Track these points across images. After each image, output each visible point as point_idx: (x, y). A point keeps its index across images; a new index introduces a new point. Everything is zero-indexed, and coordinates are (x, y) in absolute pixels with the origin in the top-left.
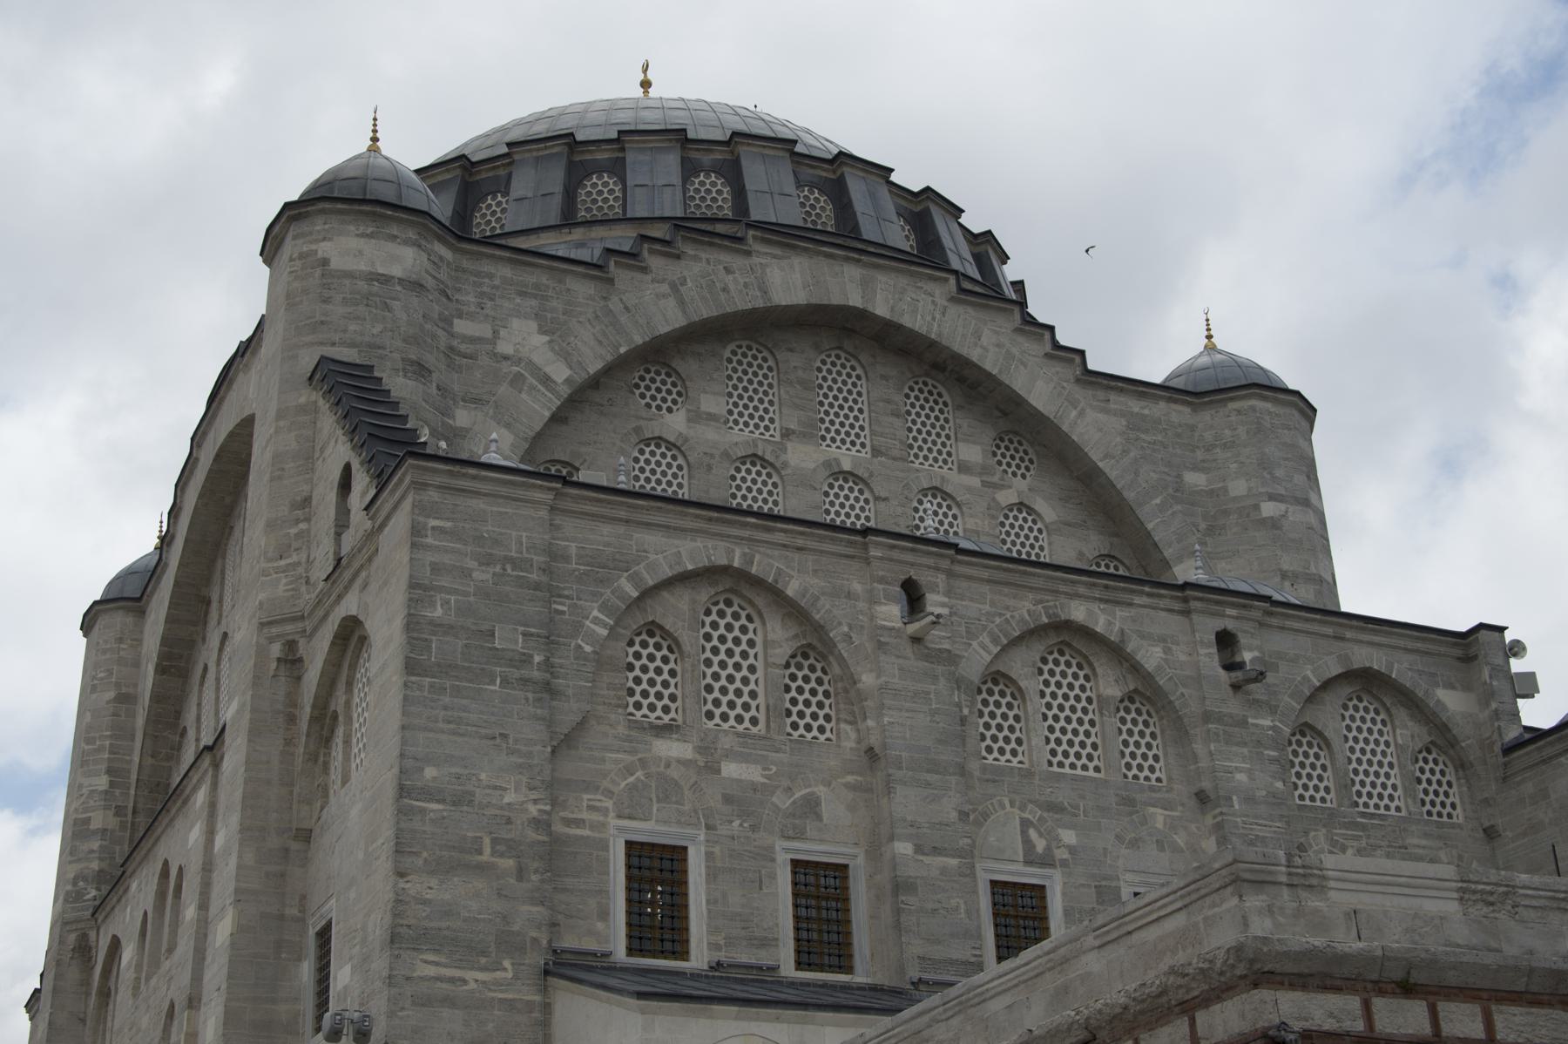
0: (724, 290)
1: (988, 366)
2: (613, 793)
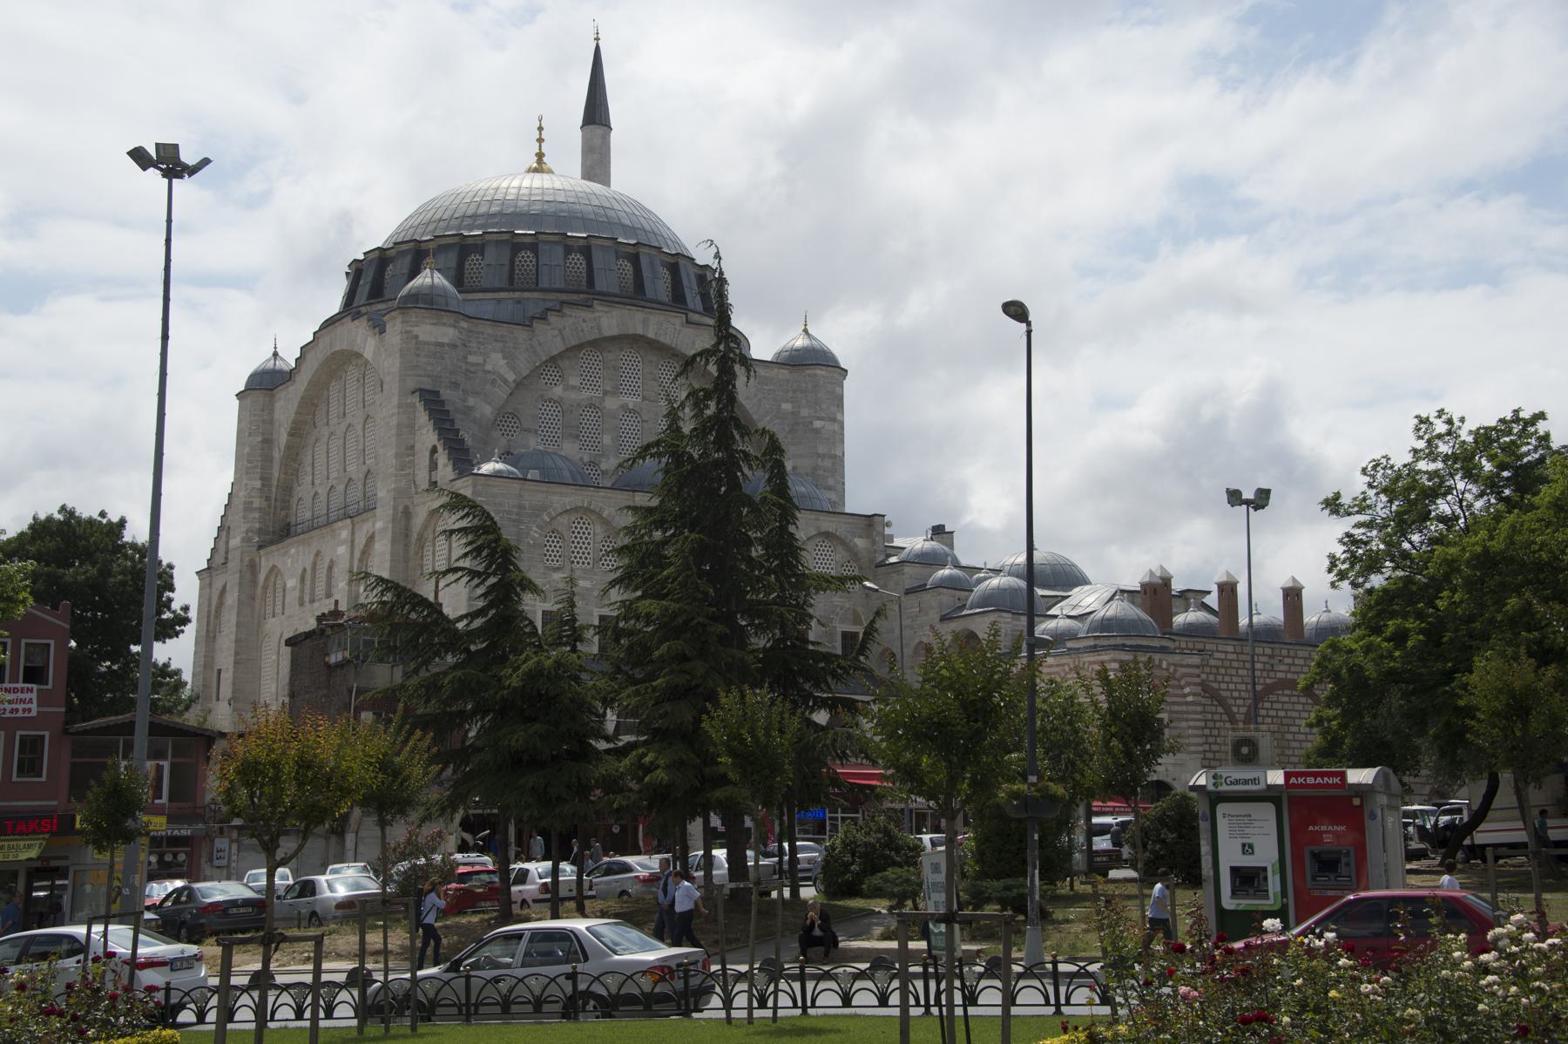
0: (583, 331)
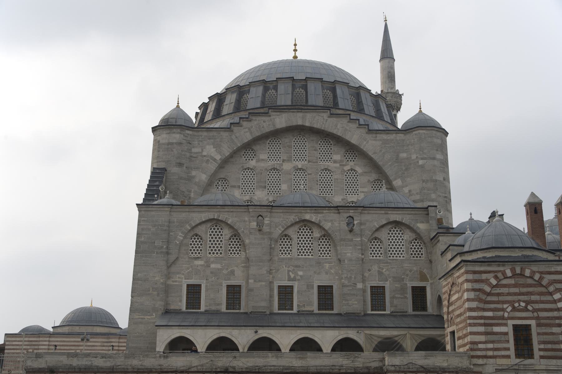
1: (339, 134)
2: (184, 274)
